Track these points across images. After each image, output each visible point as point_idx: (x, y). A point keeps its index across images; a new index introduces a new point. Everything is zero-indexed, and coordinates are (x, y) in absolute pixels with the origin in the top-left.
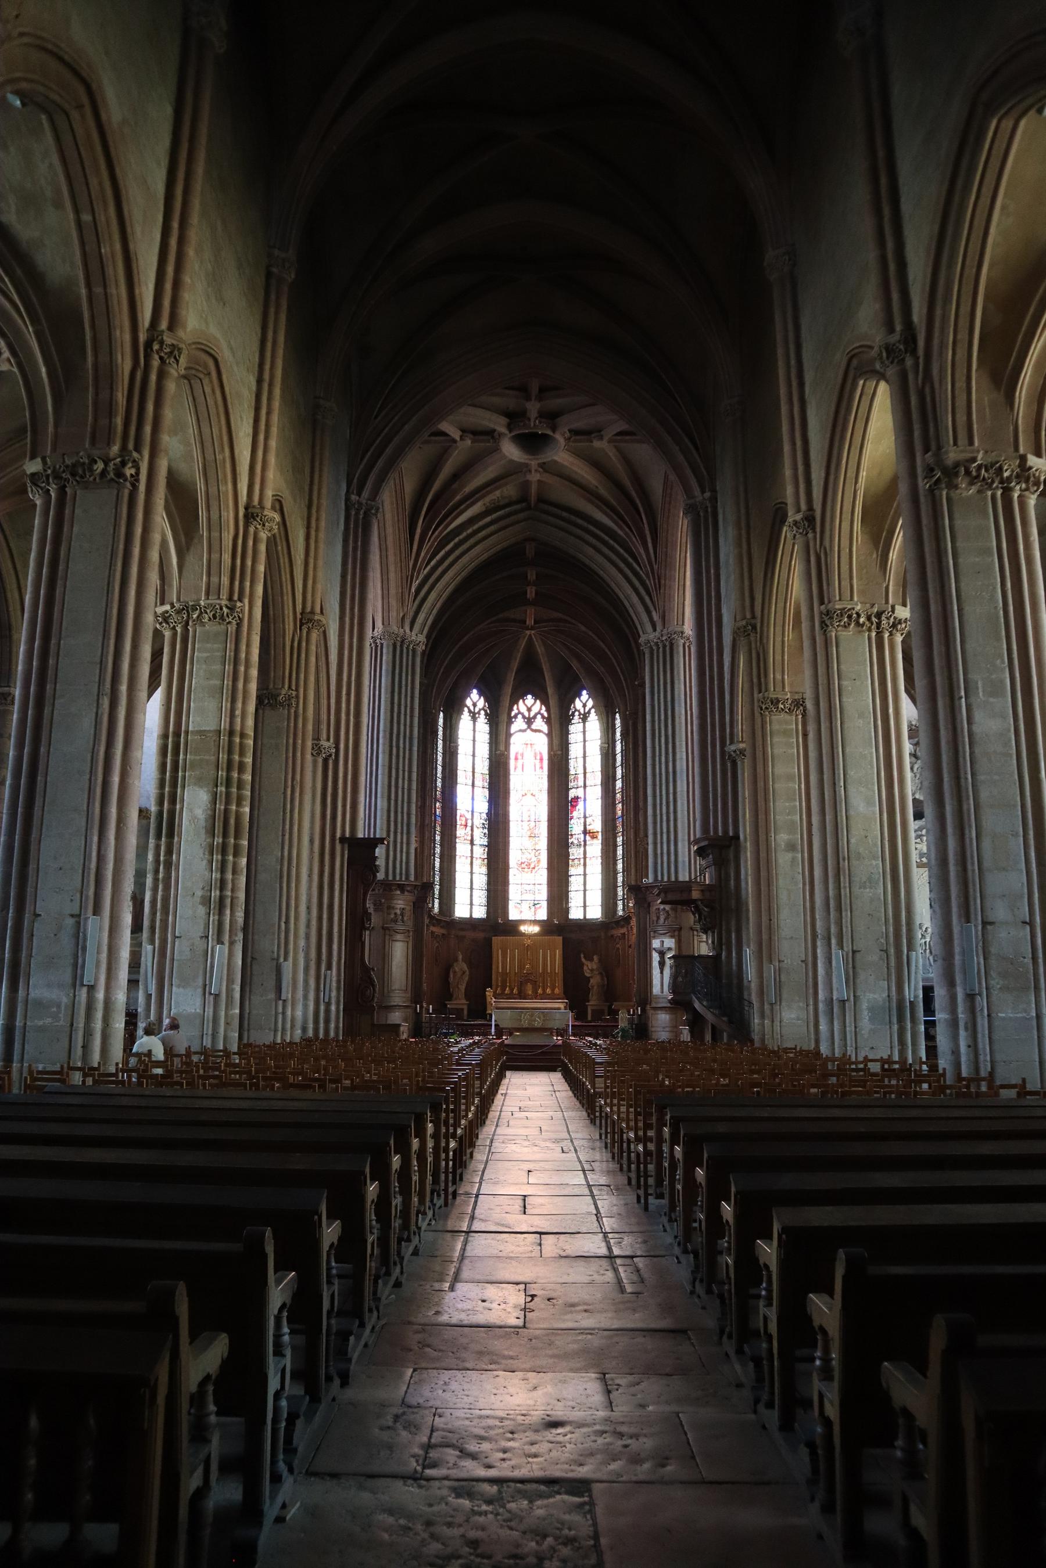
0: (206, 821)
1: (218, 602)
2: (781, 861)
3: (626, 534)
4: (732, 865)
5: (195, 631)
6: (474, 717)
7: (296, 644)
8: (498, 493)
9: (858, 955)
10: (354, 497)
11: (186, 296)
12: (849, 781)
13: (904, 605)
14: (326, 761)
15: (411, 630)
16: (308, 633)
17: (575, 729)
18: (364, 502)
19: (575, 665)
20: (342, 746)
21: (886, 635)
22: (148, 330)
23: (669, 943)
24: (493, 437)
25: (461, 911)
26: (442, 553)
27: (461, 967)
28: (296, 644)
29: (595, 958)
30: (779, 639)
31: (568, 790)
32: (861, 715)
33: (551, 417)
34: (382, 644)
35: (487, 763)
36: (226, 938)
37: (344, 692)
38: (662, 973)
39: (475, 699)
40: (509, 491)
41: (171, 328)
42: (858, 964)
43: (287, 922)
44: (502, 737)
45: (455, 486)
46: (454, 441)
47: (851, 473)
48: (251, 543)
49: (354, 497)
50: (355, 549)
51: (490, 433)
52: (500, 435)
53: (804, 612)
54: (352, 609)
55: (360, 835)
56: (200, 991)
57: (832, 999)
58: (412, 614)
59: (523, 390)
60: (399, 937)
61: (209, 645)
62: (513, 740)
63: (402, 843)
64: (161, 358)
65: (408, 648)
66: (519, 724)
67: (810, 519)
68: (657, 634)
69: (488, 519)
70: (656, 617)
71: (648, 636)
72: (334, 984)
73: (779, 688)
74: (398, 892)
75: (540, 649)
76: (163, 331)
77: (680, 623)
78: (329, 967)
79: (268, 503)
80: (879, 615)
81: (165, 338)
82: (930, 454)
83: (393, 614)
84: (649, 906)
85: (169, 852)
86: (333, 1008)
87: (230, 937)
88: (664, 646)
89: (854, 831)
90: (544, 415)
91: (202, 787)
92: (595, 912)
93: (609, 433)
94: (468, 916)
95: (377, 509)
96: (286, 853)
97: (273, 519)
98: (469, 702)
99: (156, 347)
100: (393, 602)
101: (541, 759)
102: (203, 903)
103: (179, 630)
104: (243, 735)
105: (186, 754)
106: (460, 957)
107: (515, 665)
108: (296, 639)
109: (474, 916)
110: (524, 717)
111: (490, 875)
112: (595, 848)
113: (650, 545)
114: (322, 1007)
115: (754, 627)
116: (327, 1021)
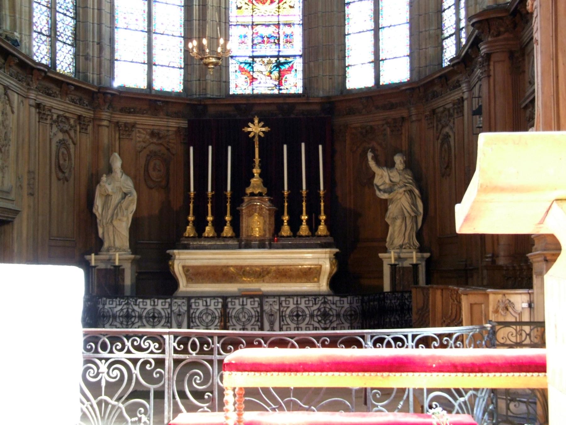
94: (142, 84)
109: (157, 86)
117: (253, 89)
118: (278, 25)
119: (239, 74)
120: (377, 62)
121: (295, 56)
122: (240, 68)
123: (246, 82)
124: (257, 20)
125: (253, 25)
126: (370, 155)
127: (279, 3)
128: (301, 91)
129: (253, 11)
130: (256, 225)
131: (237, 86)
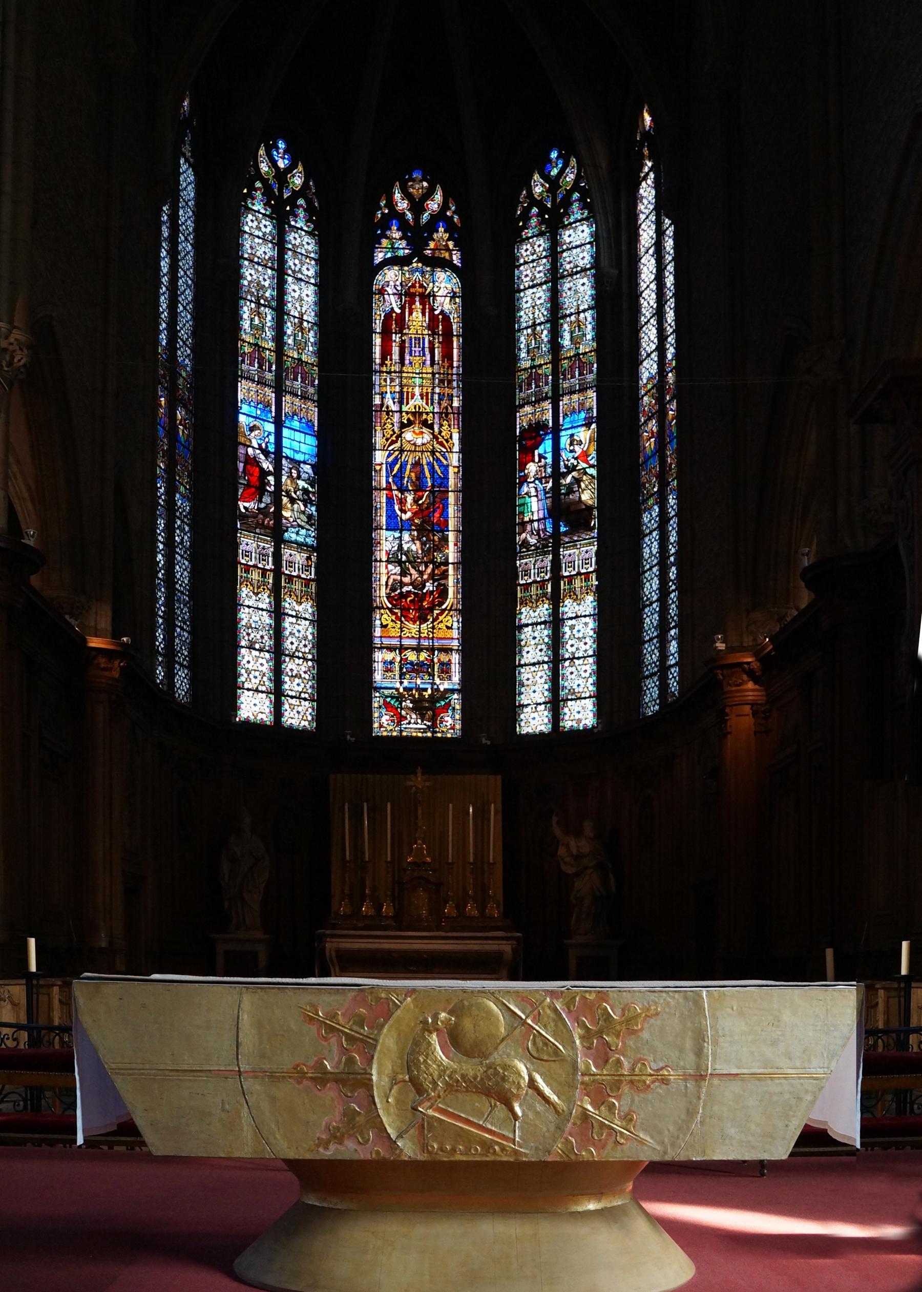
6: (281, 217)
17: (532, 251)
66: (395, 241)
92: (581, 714)
110: (404, 226)
111: (321, 622)
112: (581, 555)
117: (401, 731)
118: (431, 650)
119: (384, 711)
120: (556, 703)
121: (453, 691)
122: (385, 702)
123: (393, 721)
124: (406, 642)
125: (402, 649)
127: (432, 623)
128: (459, 733)
129: (402, 631)
131: (381, 726)
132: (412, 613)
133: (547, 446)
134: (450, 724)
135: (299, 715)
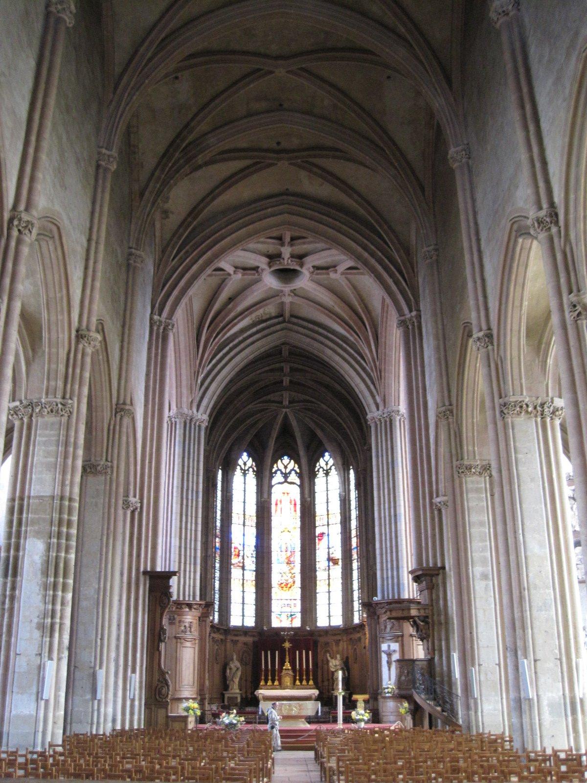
0: (42, 565)
1: (55, 400)
2: (477, 588)
3: (355, 339)
4: (441, 589)
5: (37, 421)
6: (245, 473)
7: (112, 427)
8: (261, 311)
9: (538, 662)
10: (156, 317)
11: (38, 187)
12: (526, 530)
13: (560, 397)
14: (133, 512)
15: (198, 411)
16: (121, 419)
17: (320, 481)
18: (163, 320)
19: (319, 433)
20: (145, 501)
21: (548, 420)
22: (11, 211)
23: (395, 646)
24: (257, 272)
25: (235, 621)
26: (221, 354)
27: (235, 664)
28: (112, 427)
29: (338, 656)
30: (470, 421)
31: (315, 527)
32: (533, 480)
33: (300, 257)
34: (176, 422)
35: (254, 507)
36: (55, 655)
37: (147, 461)
38: (389, 669)
39: (245, 460)
40: (270, 309)
41: (27, 209)
42: (538, 670)
43: (102, 639)
44: (266, 488)
45: (230, 306)
46: (229, 275)
47: (517, 303)
48: (79, 356)
49: (156, 317)
50: (156, 355)
51: (256, 269)
52: (263, 270)
53: (488, 404)
54: (154, 399)
55: (159, 569)
56: (34, 697)
57: (520, 698)
58: (198, 399)
59: (280, 239)
60: (188, 644)
61: (47, 432)
62: (274, 490)
63: (190, 571)
64: (19, 231)
65: (195, 425)
66: (278, 478)
67: (489, 336)
68: (380, 412)
69: (254, 330)
70: (378, 399)
71: (373, 414)
72: (137, 684)
73: (471, 457)
74: (187, 610)
75: (294, 423)
76: (21, 212)
77: (397, 404)
78: (134, 671)
79: (93, 328)
80: (542, 405)
81: (22, 216)
82: (572, 294)
83: (184, 399)
84: (378, 618)
85: (13, 588)
86: (137, 703)
87: (58, 654)
88: (386, 422)
89: (531, 568)
90: (292, 256)
91: (39, 539)
92: (337, 621)
93: (341, 268)
94: (241, 625)
95: (173, 326)
96: (102, 586)
97: (95, 339)
98: (240, 462)
99: (16, 222)
100: (185, 391)
101: (295, 505)
102: (38, 628)
103: (26, 420)
104: (71, 500)
105: (28, 513)
106: (235, 657)
107: (274, 435)
108: (112, 423)
109: (245, 624)
110: (282, 473)
112: (337, 571)
113: (373, 347)
114: (128, 703)
115: (451, 412)
116: (132, 714)
126: (328, 655)
130: (287, 680)
132: (285, 589)
133: (325, 538)
134: (297, 623)
135: (250, 622)
